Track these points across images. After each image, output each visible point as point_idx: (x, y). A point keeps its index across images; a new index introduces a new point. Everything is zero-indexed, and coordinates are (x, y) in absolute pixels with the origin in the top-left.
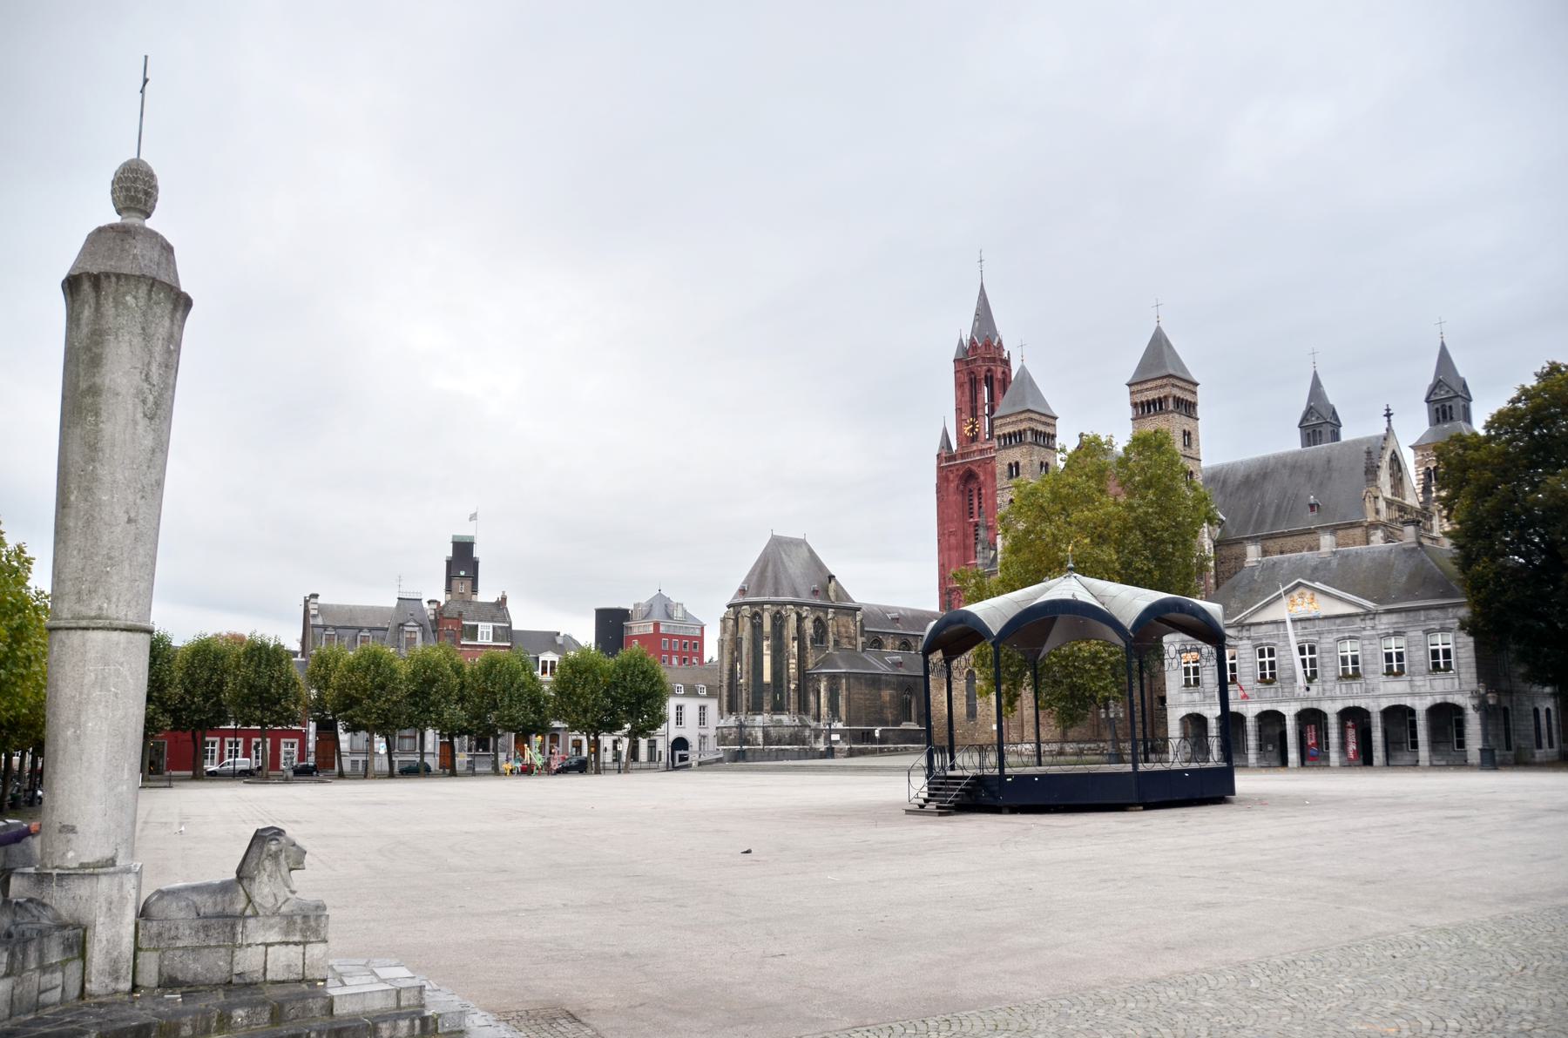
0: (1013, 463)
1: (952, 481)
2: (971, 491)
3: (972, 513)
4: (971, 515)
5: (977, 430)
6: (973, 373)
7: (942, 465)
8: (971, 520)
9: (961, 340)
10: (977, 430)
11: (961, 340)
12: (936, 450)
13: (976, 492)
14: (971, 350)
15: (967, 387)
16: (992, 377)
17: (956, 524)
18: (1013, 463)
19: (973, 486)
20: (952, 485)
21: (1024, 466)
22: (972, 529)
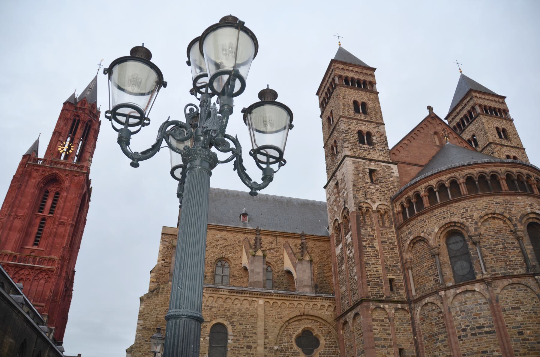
0: (360, 102)
1: (34, 178)
2: (47, 192)
3: (43, 209)
4: (41, 210)
5: (70, 151)
6: (78, 116)
7: (28, 162)
8: (40, 214)
9: (74, 95)
10: (70, 151)
11: (74, 95)
12: (25, 149)
13: (52, 194)
14: (80, 103)
15: (70, 123)
16: (90, 127)
17: (26, 211)
18: (360, 102)
19: (53, 189)
20: (34, 181)
21: (373, 109)
22: (38, 221)
